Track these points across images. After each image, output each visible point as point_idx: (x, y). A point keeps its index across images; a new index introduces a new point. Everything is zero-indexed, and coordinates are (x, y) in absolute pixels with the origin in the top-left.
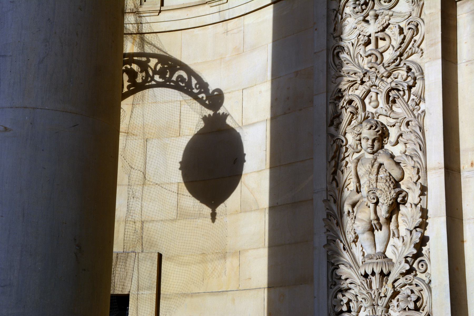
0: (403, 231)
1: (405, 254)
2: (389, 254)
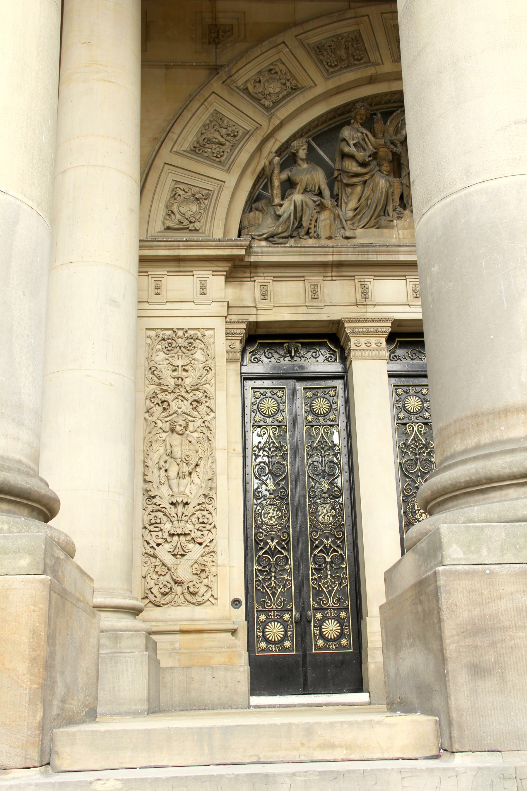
2: (187, 492)
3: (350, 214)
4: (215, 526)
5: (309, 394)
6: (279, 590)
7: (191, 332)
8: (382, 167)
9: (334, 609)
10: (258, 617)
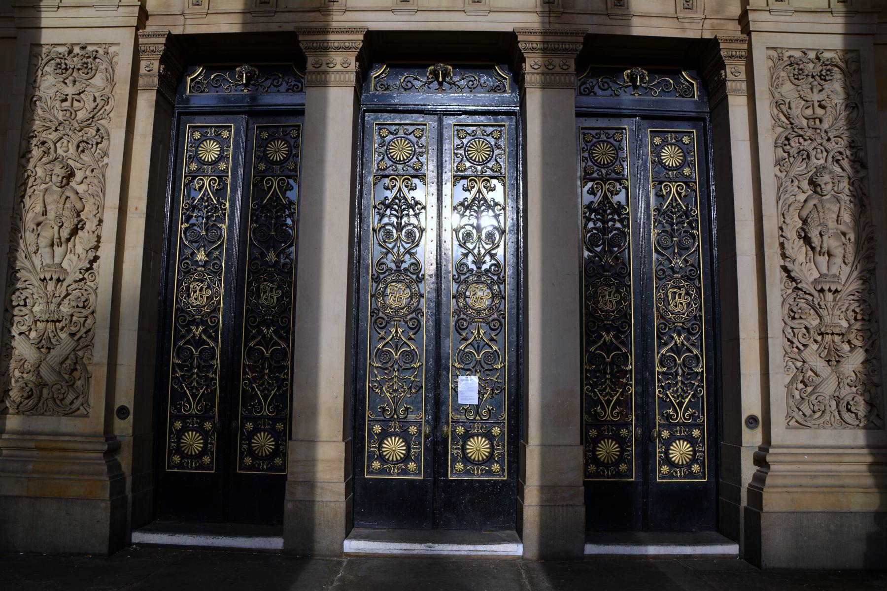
0: (79, 249)
1: (80, 267)
2: (64, 265)
4: (93, 313)
5: (265, 135)
6: (201, 391)
7: (90, 49)
9: (269, 420)
10: (172, 424)
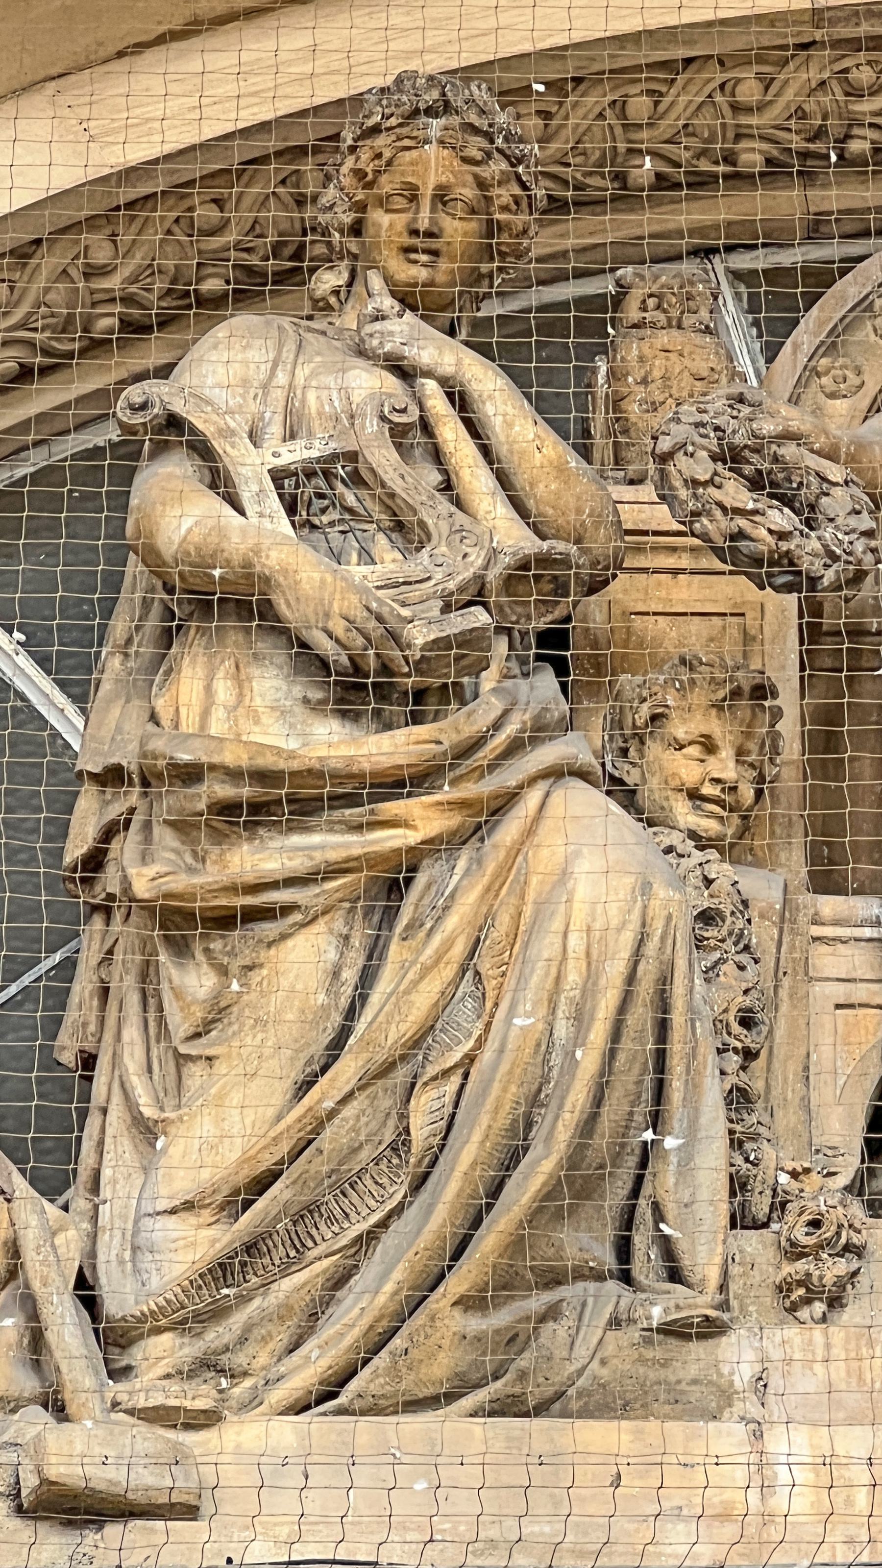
3: (190, 1246)
8: (654, 749)
